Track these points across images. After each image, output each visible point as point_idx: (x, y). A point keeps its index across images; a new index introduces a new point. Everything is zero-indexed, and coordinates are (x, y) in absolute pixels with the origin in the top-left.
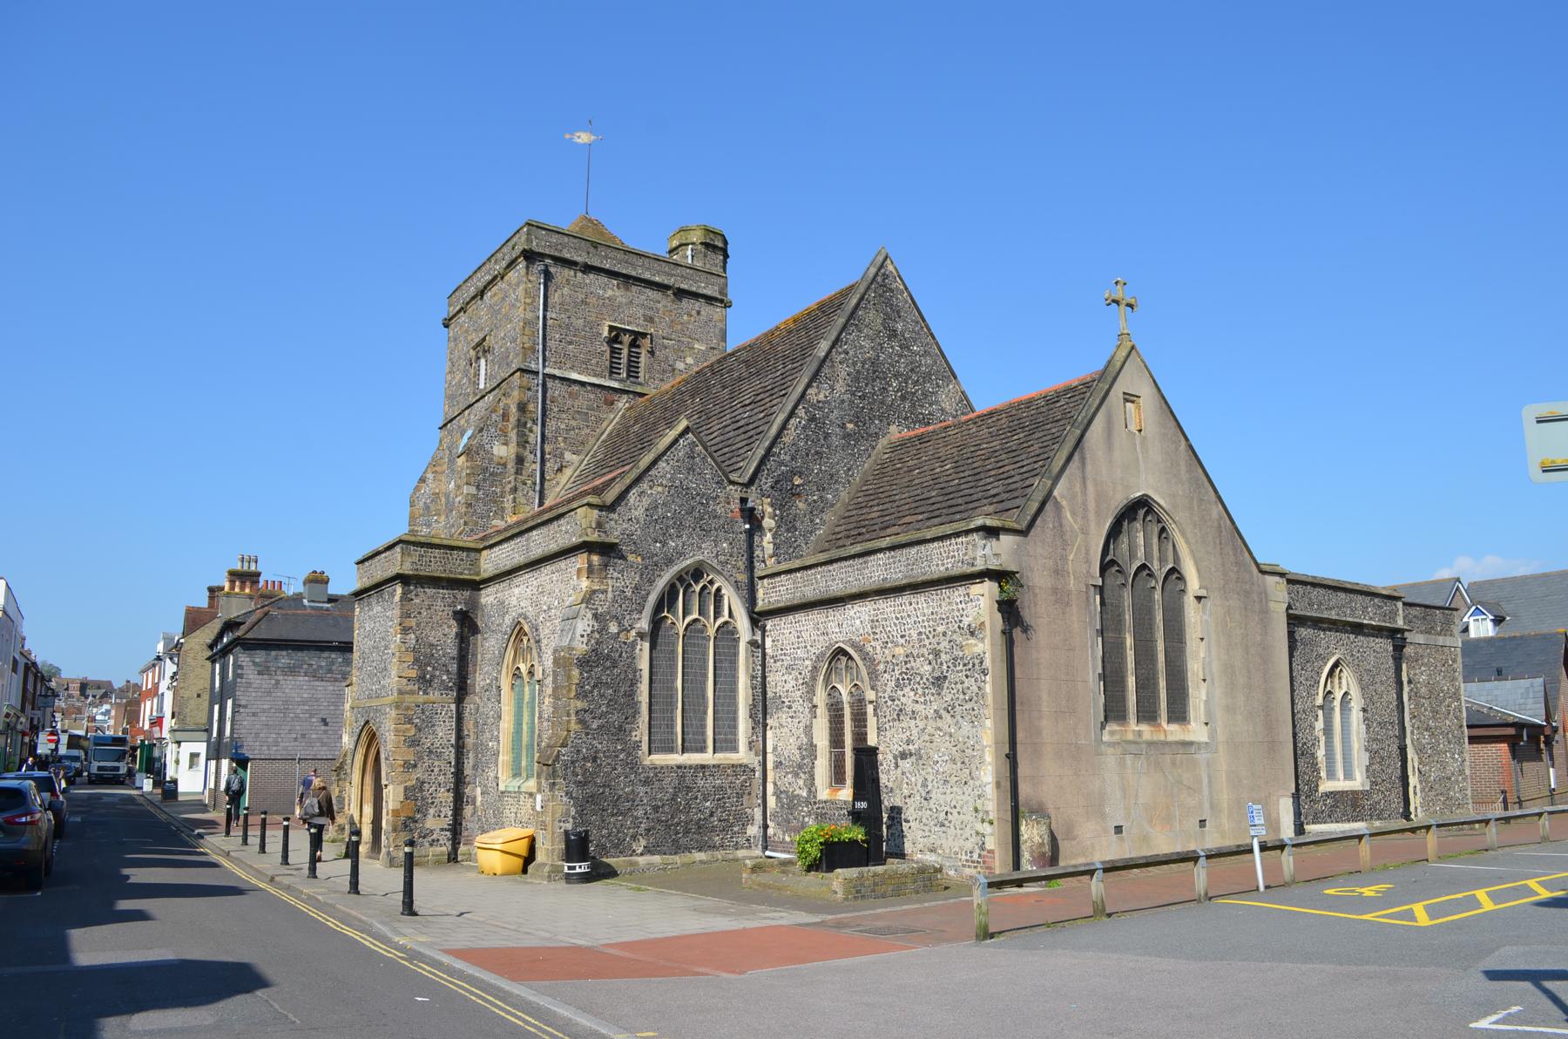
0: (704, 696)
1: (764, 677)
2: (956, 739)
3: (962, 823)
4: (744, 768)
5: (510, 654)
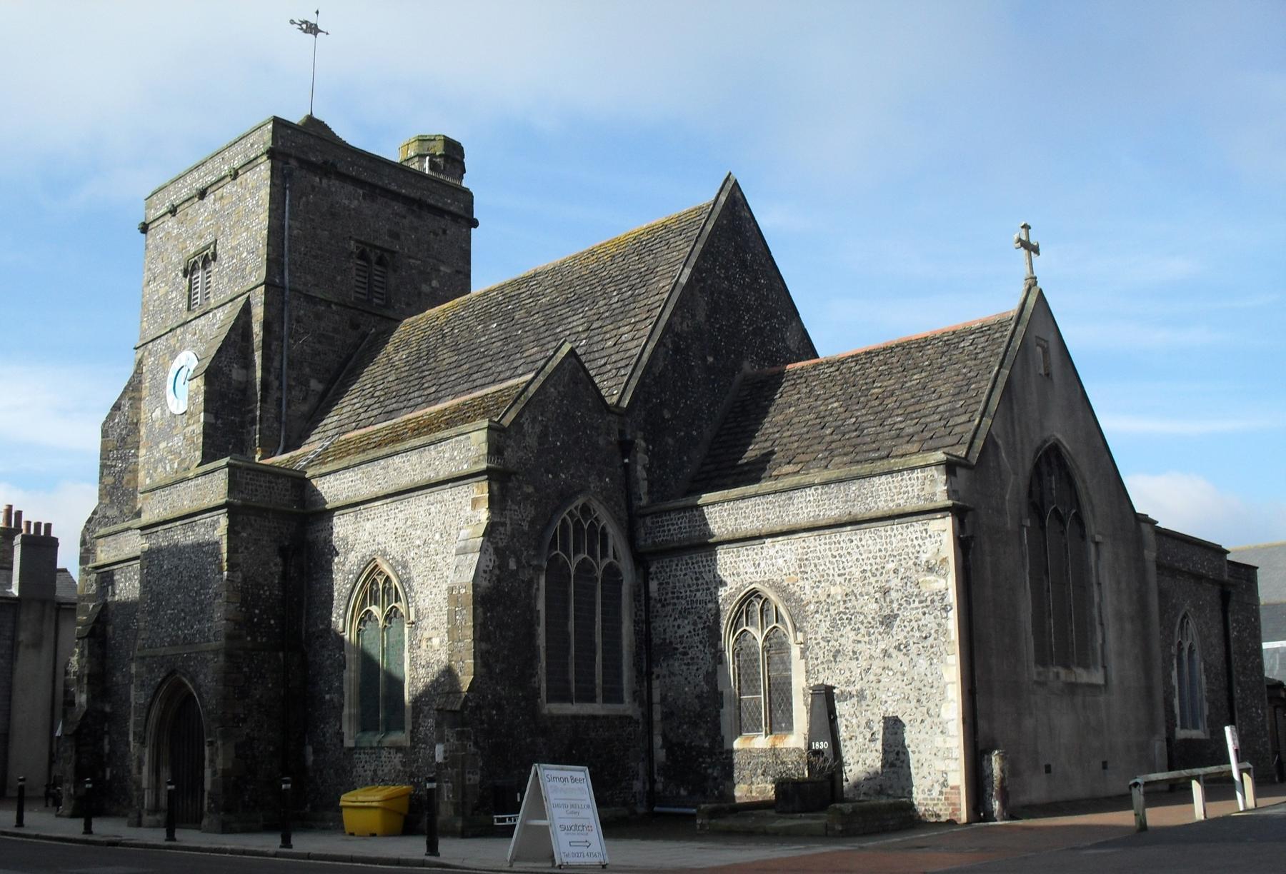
0: (593, 643)
1: (648, 623)
2: (910, 678)
3: (918, 761)
4: (629, 718)
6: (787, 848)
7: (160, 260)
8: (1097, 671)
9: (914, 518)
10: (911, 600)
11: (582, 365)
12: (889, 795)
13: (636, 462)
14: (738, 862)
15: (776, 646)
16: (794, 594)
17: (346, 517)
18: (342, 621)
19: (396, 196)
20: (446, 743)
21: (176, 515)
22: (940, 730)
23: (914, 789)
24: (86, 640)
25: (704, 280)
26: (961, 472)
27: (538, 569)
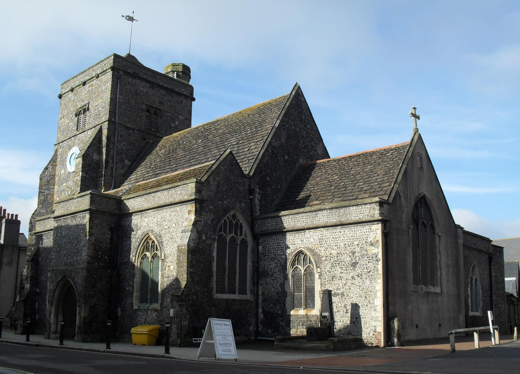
0: (236, 270)
1: (258, 262)
3: (365, 322)
6: (310, 355)
7: (66, 110)
8: (438, 287)
9: (366, 224)
10: (364, 257)
11: (235, 158)
12: (353, 335)
13: (255, 198)
14: (291, 360)
15: (309, 274)
16: (317, 253)
17: (137, 216)
18: (134, 258)
19: (162, 87)
20: (175, 309)
21: (68, 213)
22: (374, 309)
23: (363, 333)
24: (30, 262)
25: (285, 125)
26: (385, 206)
27: (214, 239)
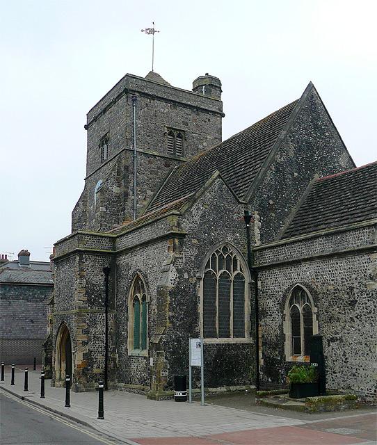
1: (257, 301)
5: (132, 288)
13: (254, 226)
19: (186, 106)
